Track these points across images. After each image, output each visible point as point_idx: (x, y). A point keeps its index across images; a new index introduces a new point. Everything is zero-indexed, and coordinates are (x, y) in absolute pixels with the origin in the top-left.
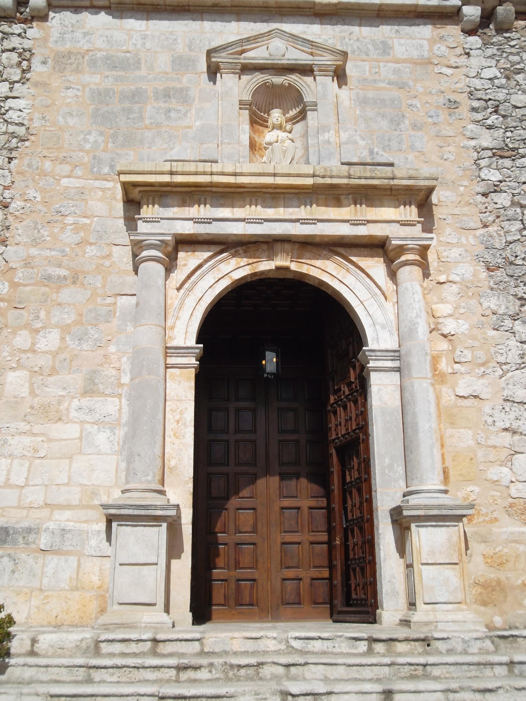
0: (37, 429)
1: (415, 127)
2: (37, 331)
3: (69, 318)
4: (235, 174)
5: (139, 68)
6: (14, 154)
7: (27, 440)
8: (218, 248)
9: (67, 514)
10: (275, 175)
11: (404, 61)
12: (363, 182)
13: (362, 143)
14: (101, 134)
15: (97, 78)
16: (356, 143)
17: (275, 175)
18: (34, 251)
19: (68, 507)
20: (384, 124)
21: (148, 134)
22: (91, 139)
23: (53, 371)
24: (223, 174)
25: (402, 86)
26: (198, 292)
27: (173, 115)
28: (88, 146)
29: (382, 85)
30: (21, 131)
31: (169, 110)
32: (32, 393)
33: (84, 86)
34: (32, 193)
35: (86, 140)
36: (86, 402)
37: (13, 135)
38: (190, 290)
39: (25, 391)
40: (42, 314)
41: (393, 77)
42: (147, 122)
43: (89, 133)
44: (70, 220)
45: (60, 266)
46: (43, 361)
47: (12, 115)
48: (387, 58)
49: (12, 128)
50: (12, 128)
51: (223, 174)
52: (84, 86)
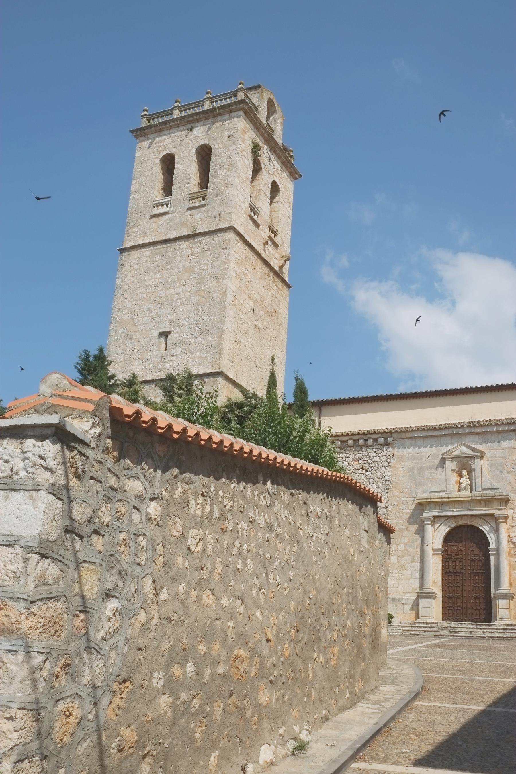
0: (400, 572)
1: (508, 473)
2: (398, 545)
3: (406, 541)
4: (448, 498)
5: (422, 459)
6: (388, 491)
7: (397, 575)
8: (445, 519)
9: (409, 595)
10: (460, 497)
11: (505, 449)
12: (486, 498)
13: (489, 482)
14: (412, 482)
15: (409, 464)
16: (487, 482)
17: (460, 497)
18: (395, 521)
19: (409, 593)
20: (498, 472)
21: (425, 481)
22: (409, 484)
23: (403, 556)
24: (445, 498)
25: (504, 458)
26: (441, 532)
27: (433, 474)
28: (408, 487)
29: (498, 458)
30: (389, 483)
31: (431, 473)
32: (398, 562)
33: (406, 467)
34: (394, 503)
35: (408, 485)
36: (412, 564)
37: (387, 484)
38: (439, 531)
39: (396, 562)
40: (399, 540)
41: (501, 455)
42: (425, 477)
43: (408, 483)
44: (405, 511)
45: (403, 525)
46: (400, 553)
47: (386, 478)
48: (500, 448)
49: (387, 482)
50: (387, 482)
51: (445, 498)
52: (406, 467)
